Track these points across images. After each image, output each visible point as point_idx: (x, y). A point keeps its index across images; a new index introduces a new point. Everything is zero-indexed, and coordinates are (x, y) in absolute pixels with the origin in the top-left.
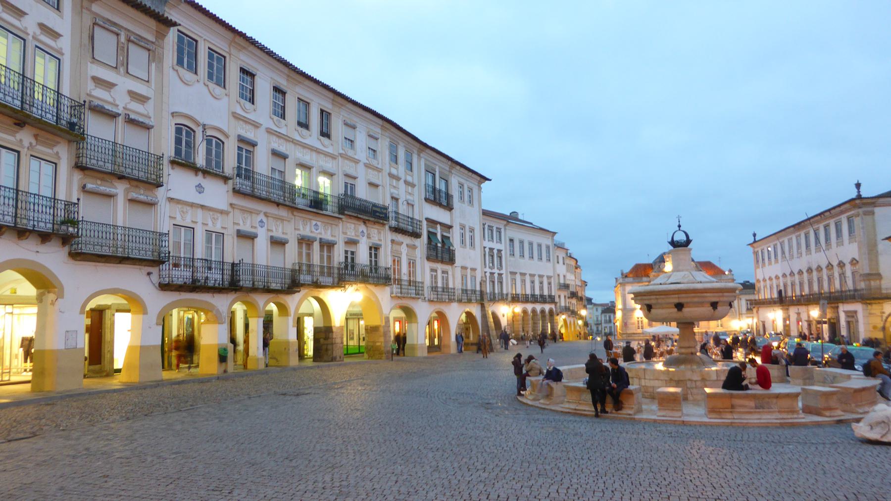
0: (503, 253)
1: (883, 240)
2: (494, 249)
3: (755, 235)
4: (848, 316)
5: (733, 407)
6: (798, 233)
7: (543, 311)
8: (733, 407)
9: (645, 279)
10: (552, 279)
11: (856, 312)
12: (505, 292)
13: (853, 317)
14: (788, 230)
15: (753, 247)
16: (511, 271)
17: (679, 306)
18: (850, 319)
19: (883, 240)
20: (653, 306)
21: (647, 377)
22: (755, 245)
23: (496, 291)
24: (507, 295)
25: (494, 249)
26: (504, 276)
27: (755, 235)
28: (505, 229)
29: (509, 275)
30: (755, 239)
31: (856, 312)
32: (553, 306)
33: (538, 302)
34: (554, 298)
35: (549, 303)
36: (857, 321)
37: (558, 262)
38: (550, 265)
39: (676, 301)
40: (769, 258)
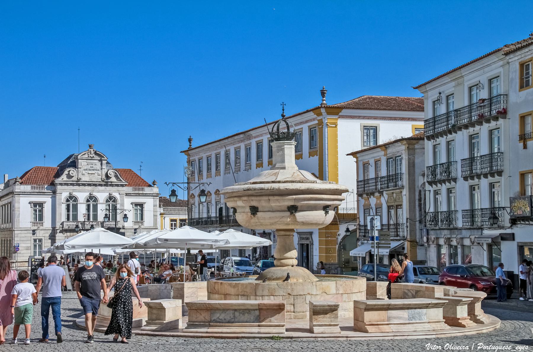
1: (347, 155)
3: (190, 140)
4: (301, 239)
5: (389, 319)
6: (249, 142)
8: (389, 319)
11: (311, 233)
13: (307, 239)
14: (236, 137)
15: (189, 155)
17: (293, 209)
18: (305, 242)
19: (347, 155)
20: (259, 210)
21: (258, 294)
22: (189, 152)
27: (190, 140)
30: (190, 145)
31: (311, 233)
36: (312, 244)
39: (292, 203)
40: (209, 169)
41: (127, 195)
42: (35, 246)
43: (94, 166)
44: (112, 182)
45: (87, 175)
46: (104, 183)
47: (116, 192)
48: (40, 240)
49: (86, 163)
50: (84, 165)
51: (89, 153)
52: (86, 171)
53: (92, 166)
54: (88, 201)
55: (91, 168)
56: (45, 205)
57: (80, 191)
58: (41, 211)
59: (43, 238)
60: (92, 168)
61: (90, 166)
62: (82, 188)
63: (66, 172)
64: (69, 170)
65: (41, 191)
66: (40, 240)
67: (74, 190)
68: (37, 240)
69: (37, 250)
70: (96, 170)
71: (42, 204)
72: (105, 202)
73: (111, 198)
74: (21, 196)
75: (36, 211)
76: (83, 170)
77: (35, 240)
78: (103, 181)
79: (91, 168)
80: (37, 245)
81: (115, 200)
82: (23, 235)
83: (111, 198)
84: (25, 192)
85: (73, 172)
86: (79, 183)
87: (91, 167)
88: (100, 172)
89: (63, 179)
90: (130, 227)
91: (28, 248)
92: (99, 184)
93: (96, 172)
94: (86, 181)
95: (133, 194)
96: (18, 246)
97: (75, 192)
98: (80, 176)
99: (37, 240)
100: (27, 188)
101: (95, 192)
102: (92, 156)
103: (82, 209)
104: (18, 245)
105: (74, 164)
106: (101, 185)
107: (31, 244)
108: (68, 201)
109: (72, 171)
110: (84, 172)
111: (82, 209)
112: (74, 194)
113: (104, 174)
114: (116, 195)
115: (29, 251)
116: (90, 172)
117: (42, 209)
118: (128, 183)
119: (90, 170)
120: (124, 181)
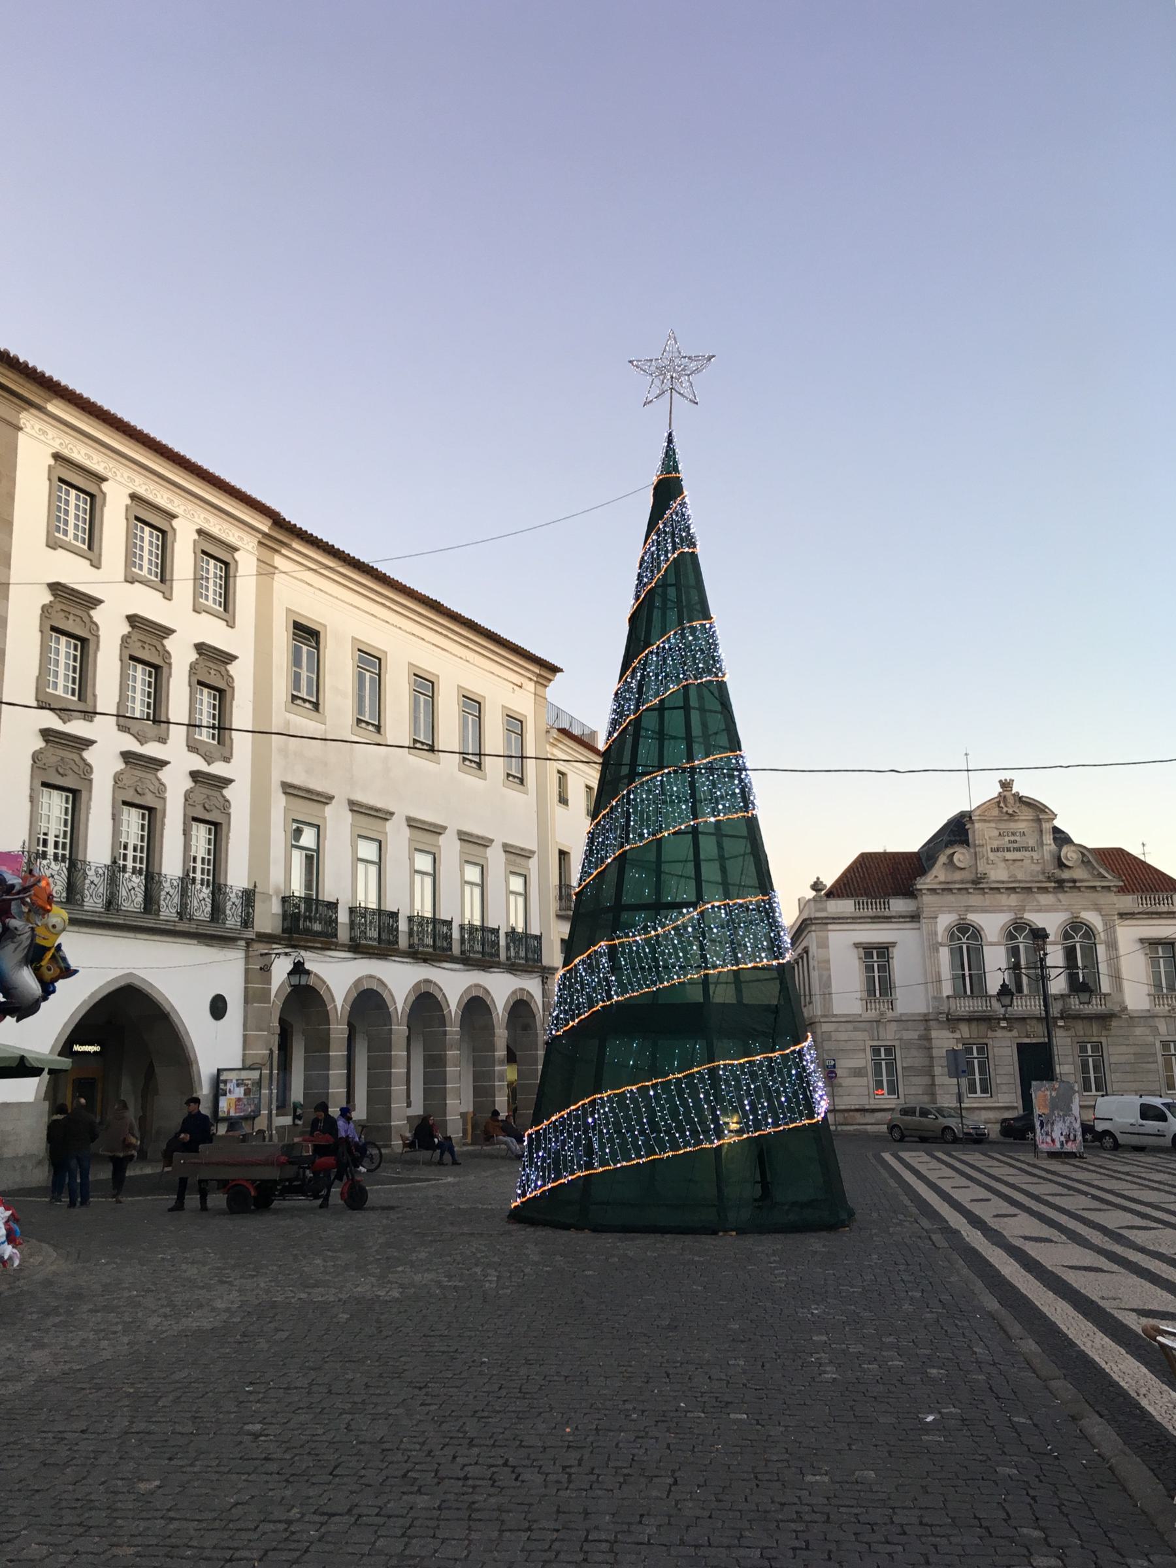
0: (242, 674)
2: (169, 632)
7: (476, 1005)
9: (898, 905)
10: (533, 863)
12: (237, 878)
16: (290, 780)
23: (171, 866)
24: (249, 897)
25: (169, 632)
26: (239, 797)
28: (266, 570)
29: (279, 801)
32: (532, 985)
33: (453, 959)
34: (538, 950)
35: (512, 968)
37: (563, 801)
38: (521, 803)
41: (1122, 915)
42: (877, 1066)
43: (1018, 838)
44: (1074, 881)
45: (1003, 865)
46: (1053, 885)
47: (1085, 909)
48: (889, 1050)
49: (996, 833)
50: (990, 838)
51: (1002, 805)
52: (999, 854)
53: (1012, 838)
54: (1010, 936)
55: (1010, 845)
56: (896, 953)
57: (984, 910)
58: (885, 968)
59: (896, 1043)
60: (1015, 845)
61: (1007, 839)
62: (988, 900)
63: (942, 859)
64: (951, 851)
65: (880, 914)
66: (889, 1050)
67: (970, 909)
68: (882, 1050)
69: (885, 1078)
70: (1026, 849)
71: (887, 948)
72: (1060, 939)
73: (1076, 927)
74: (830, 927)
75: (869, 968)
76: (989, 850)
77: (876, 1050)
78: (1049, 879)
79: (1010, 845)
80: (883, 1063)
81: (1090, 933)
82: (843, 1036)
83: (1076, 927)
84: (839, 918)
85: (962, 858)
86: (981, 886)
87: (1010, 842)
88: (1035, 855)
89: (936, 877)
90: (1142, 1010)
91: (858, 1072)
92: (1039, 888)
93: (1027, 854)
94: (1003, 882)
95: (1139, 913)
96: (834, 1066)
97: (973, 912)
98: (982, 867)
99: (882, 1050)
100: (845, 906)
101: (1030, 911)
102: (1010, 811)
103: (995, 960)
104: (833, 1063)
105: (963, 838)
106: (1044, 890)
107: (864, 1060)
108: (952, 936)
109: (961, 856)
110: (992, 856)
111: (995, 960)
112: (973, 918)
113: (1047, 856)
114: (1093, 918)
115: (863, 1081)
116: (1009, 856)
117: (888, 961)
118: (1123, 881)
119: (1009, 850)
120: (1110, 877)
